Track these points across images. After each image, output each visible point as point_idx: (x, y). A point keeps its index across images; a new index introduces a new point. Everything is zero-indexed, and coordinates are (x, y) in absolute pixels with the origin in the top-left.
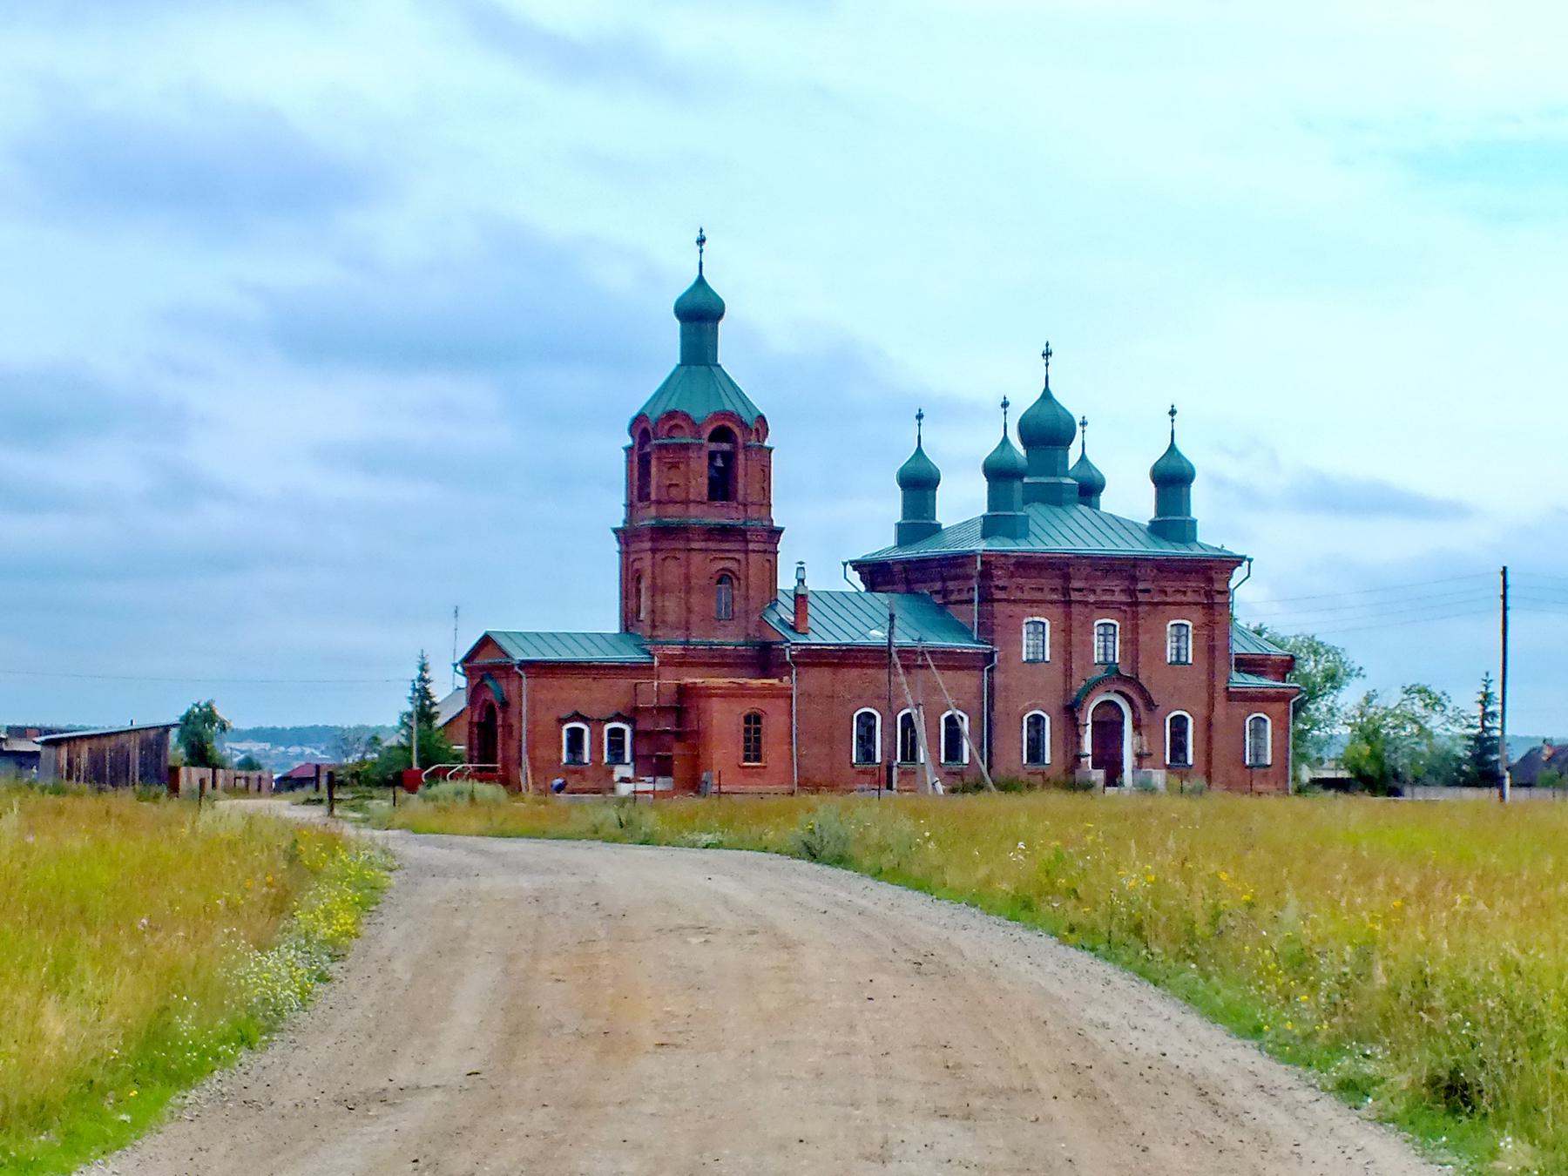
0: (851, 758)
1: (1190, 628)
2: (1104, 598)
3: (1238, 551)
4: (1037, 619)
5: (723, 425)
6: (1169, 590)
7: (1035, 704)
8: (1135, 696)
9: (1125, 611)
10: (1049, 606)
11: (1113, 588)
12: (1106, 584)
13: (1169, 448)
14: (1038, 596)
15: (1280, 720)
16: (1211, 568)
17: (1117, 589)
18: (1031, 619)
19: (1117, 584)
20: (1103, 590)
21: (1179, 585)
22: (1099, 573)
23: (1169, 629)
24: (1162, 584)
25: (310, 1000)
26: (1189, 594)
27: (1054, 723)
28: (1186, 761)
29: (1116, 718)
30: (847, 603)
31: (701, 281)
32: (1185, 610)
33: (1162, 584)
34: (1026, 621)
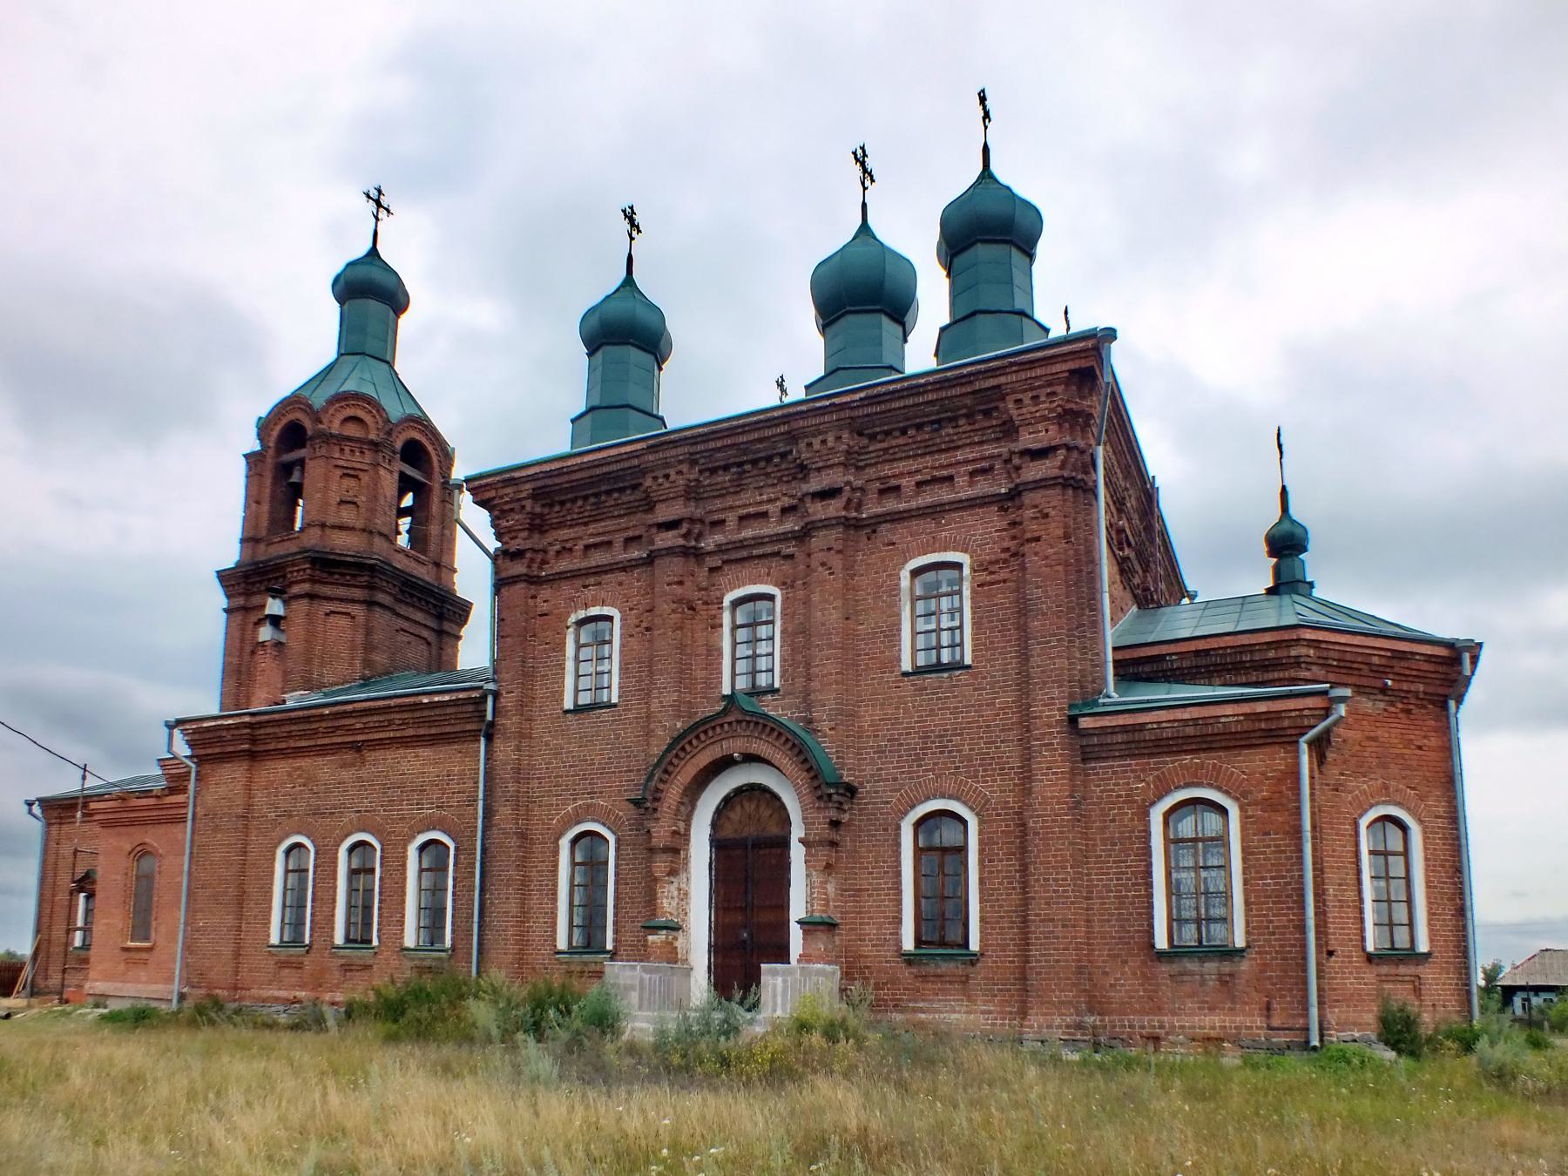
0: (1363, 939)
1: (966, 571)
2: (748, 533)
3: (1101, 323)
4: (595, 611)
5: (291, 421)
6: (907, 483)
7: (589, 806)
8: (704, 759)
9: (791, 557)
10: (622, 576)
11: (764, 508)
12: (749, 499)
13: (983, 172)
14: (599, 558)
15: (1269, 805)
16: (998, 393)
17: (773, 508)
18: (582, 614)
19: (767, 496)
20: (741, 518)
21: (927, 465)
22: (724, 478)
23: (905, 582)
24: (887, 470)
25: (1289, 1153)
26: (961, 481)
27: (628, 850)
28: (966, 945)
29: (774, 830)
30: (1297, 731)
31: (373, 252)
32: (952, 526)
33: (887, 470)
34: (573, 618)
